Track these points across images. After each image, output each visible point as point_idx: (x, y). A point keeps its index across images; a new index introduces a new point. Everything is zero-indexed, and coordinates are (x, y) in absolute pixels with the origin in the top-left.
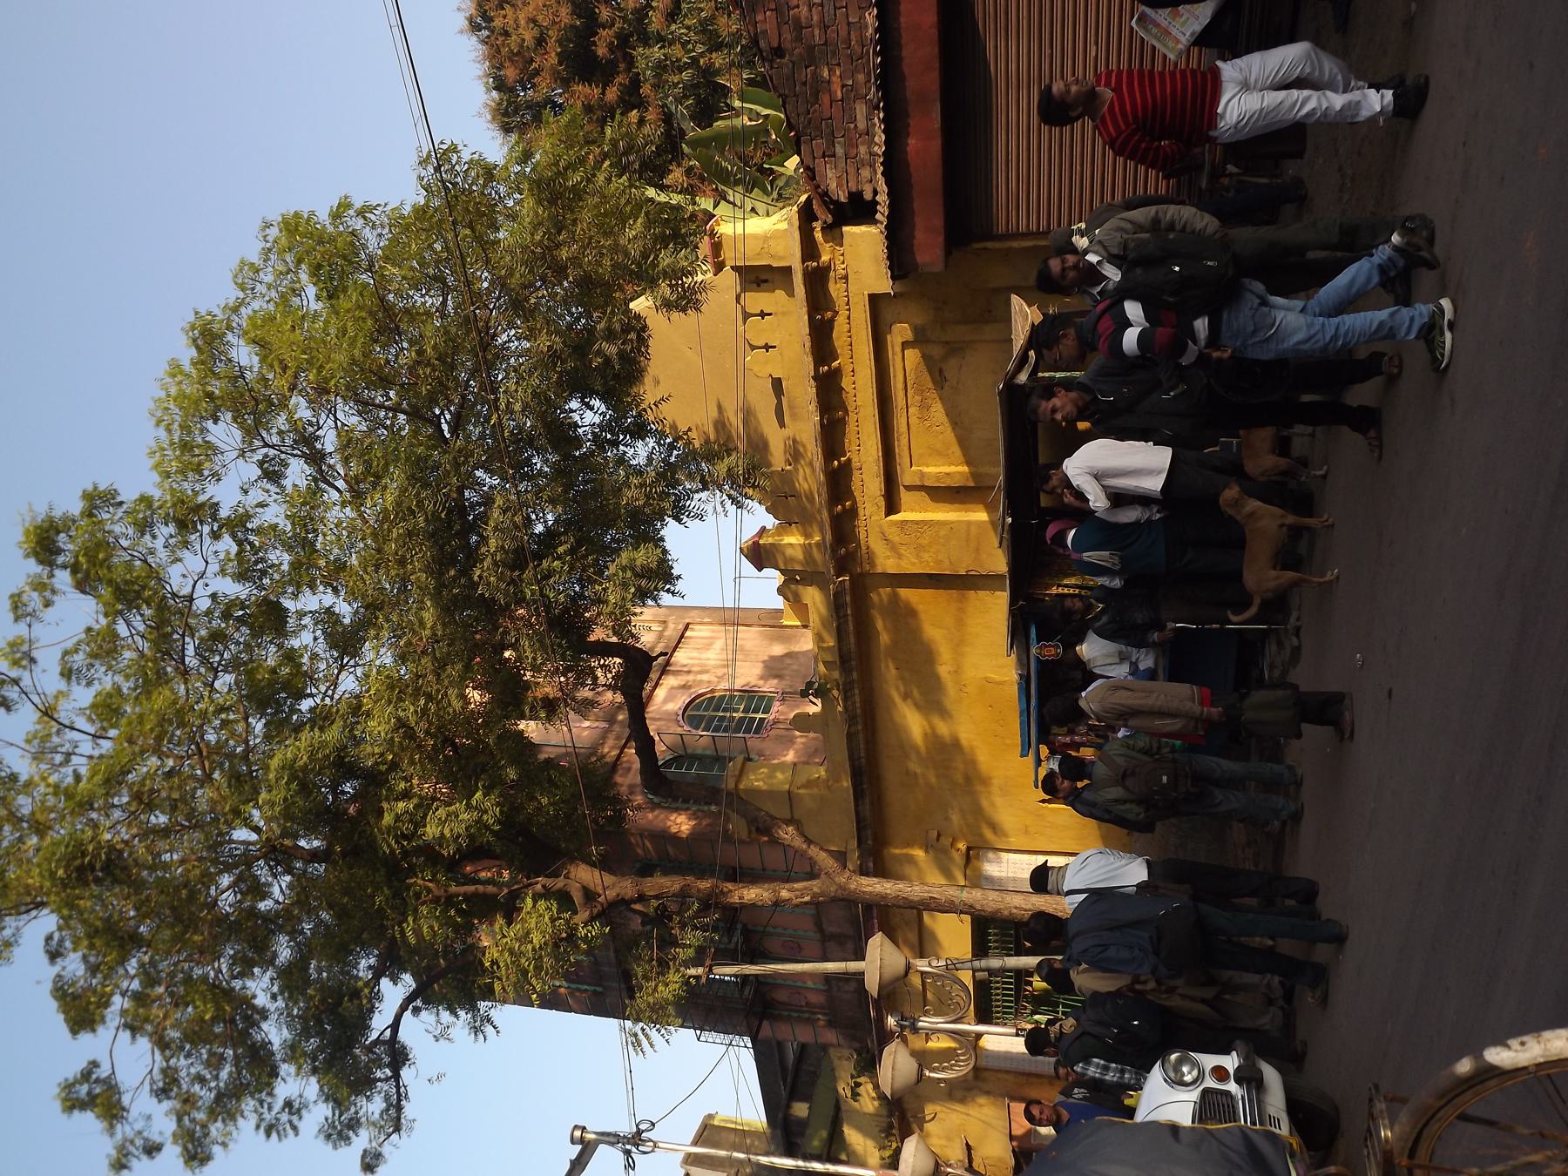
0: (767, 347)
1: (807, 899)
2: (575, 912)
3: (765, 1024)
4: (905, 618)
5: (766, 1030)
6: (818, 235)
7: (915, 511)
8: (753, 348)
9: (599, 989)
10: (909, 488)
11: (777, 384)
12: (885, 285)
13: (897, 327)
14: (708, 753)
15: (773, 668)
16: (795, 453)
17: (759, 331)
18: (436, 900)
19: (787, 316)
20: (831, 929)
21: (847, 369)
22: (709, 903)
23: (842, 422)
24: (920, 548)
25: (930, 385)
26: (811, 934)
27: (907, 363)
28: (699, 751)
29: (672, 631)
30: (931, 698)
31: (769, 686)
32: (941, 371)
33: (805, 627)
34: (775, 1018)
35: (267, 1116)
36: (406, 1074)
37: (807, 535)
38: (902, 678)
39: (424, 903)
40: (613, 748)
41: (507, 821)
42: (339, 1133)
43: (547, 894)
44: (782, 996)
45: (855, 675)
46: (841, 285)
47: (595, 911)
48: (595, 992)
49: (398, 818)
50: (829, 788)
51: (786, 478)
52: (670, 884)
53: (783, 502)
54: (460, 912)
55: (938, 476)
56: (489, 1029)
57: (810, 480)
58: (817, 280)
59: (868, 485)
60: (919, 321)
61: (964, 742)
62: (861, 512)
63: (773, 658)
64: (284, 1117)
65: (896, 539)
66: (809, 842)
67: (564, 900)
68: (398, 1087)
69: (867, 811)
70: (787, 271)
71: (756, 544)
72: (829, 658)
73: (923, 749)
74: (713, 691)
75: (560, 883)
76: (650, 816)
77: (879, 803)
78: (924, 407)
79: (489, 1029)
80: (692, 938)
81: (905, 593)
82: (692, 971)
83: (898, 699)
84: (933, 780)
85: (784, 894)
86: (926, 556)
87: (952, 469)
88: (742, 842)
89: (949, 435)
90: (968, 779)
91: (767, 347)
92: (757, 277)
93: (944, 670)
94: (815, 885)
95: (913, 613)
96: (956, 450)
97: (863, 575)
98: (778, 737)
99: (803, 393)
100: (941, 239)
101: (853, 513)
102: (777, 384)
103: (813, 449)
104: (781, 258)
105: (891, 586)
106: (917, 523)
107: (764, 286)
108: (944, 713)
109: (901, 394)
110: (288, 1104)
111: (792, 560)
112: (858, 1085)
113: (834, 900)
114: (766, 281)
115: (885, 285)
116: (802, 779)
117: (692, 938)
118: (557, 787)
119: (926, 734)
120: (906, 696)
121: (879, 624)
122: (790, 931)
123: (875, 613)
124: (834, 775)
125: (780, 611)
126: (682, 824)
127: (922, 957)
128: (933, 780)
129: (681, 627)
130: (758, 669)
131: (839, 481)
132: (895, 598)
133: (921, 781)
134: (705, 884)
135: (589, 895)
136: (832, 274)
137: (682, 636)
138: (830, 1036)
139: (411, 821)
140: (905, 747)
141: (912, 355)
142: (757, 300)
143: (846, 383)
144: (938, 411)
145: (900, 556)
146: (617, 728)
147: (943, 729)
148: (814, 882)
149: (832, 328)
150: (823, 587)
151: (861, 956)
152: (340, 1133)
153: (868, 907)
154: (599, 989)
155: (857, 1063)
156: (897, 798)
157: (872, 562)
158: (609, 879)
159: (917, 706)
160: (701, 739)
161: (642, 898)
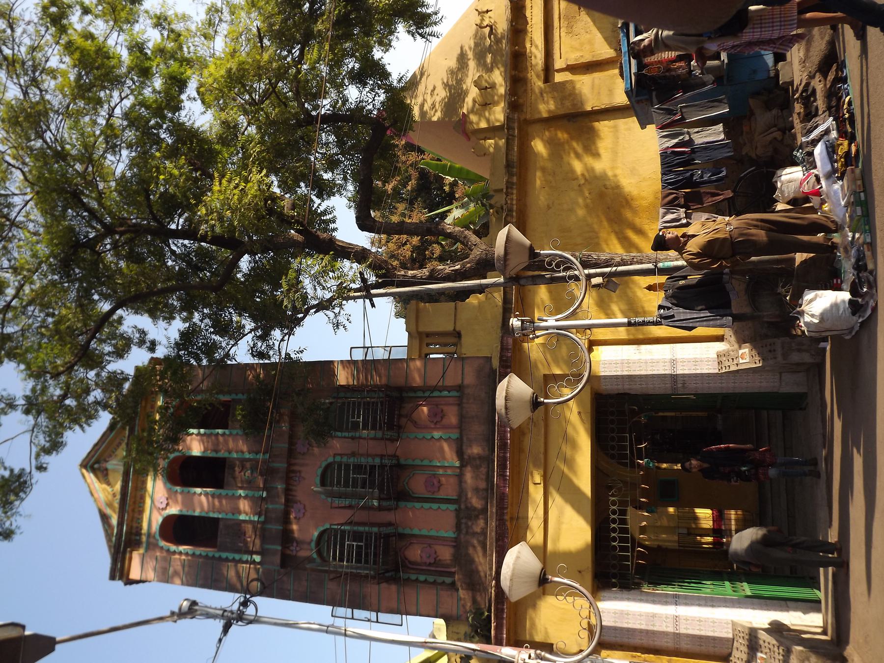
44: (415, 553)
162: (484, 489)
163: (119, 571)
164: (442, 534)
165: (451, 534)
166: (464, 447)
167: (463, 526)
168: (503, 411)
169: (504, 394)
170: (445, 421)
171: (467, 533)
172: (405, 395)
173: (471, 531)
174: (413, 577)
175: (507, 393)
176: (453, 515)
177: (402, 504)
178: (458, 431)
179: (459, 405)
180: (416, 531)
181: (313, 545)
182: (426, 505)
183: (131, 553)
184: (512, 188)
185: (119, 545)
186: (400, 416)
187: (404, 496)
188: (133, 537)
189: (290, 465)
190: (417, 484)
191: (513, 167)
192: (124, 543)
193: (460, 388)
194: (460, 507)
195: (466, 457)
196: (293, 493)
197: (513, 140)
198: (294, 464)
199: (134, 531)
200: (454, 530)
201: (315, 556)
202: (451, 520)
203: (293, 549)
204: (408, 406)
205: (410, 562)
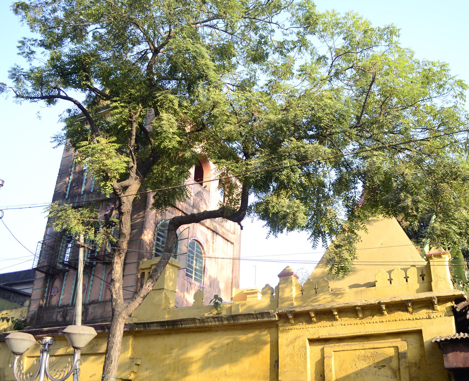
0: (390, 280)
1: (114, 296)
2: (119, 181)
3: (43, 275)
4: (255, 347)
5: (40, 275)
6: (449, 304)
7: (313, 353)
8: (390, 272)
10: (323, 350)
11: (373, 285)
12: (427, 337)
13: (405, 343)
14: (178, 251)
15: (214, 283)
16: (336, 293)
17: (398, 276)
18: (131, 117)
19: (410, 290)
21: (383, 318)
22: (115, 247)
23: (357, 316)
24: (292, 356)
25: (376, 361)
26: (88, 298)
27: (387, 349)
28: (179, 246)
29: (230, 237)
30: (209, 362)
31: (206, 280)
32: (384, 366)
33: (232, 299)
35: (29, 43)
36: (42, 103)
37: (296, 298)
38: (222, 347)
39: (130, 111)
40: (182, 206)
41: (165, 152)
42: (15, 75)
43: (129, 168)
44: (57, 283)
45: (226, 322)
46: (425, 316)
47: (118, 191)
48: (65, 194)
49: (171, 101)
50: (165, 309)
51: (325, 289)
52: (126, 229)
53: (313, 286)
54: (123, 127)
55: (330, 365)
56: (56, 144)
57: (324, 301)
58: (428, 304)
59: (324, 329)
60: (409, 355)
62: (310, 326)
63: (218, 283)
64: (27, 50)
65: (296, 344)
66: (144, 298)
67: (124, 177)
68: (38, 98)
69: (154, 328)
70: (430, 290)
71: (292, 274)
72: (233, 309)
73: (184, 357)
74: (205, 253)
75: (133, 174)
76: (152, 222)
77: (158, 334)
78: (365, 358)
79: (56, 144)
80: (100, 239)
81: (267, 349)
82: (82, 238)
84: (168, 362)
85: (117, 285)
86: (288, 359)
87: (334, 373)
88: (138, 264)
89: (351, 371)
91: (390, 280)
92: (425, 275)
93: (226, 368)
94: (121, 301)
95: (256, 351)
96: (343, 374)
97: (277, 327)
98: (184, 285)
99: (370, 297)
100: (461, 366)
101: (310, 321)
102: (373, 285)
103: (340, 302)
104: (436, 287)
105: (271, 341)
106: (305, 354)
107: (421, 277)
108: (202, 368)
109: (372, 346)
110: (33, 52)
111: (283, 291)
112: (8, 321)
113: (113, 310)
114: (423, 279)
115: (427, 337)
116: (169, 295)
117: (100, 239)
118: (179, 175)
119: (192, 358)
120: (213, 349)
121: (251, 335)
122: (90, 288)
123: (257, 332)
124: (170, 311)
125: (238, 288)
126: (148, 236)
127: (82, 355)
128: (168, 362)
129: (232, 241)
130: (214, 276)
131: (326, 314)
132: (265, 343)
133: (167, 356)
134: (125, 245)
135: (125, 188)
136: (431, 311)
137: (228, 241)
138: (34, 307)
139: (169, 107)
140: (185, 348)
141: (391, 352)
142: (413, 274)
143: (376, 318)
144: (363, 365)
145: (288, 346)
146: (191, 208)
147: (194, 367)
148: (122, 300)
149: (403, 311)
150: (270, 306)
151: (85, 322)
152: (15, 75)
153: (109, 327)
155: (19, 321)
156: (158, 344)
157: (283, 331)
158: (131, 198)
159: (207, 354)
160: (183, 247)
161: (121, 214)
164: (62, 297)
166: (92, 305)
171: (58, 312)
178: (102, 300)
180: (64, 282)
184: (219, 321)
191: (234, 320)
194: (70, 306)
197: (254, 318)
205: (53, 282)
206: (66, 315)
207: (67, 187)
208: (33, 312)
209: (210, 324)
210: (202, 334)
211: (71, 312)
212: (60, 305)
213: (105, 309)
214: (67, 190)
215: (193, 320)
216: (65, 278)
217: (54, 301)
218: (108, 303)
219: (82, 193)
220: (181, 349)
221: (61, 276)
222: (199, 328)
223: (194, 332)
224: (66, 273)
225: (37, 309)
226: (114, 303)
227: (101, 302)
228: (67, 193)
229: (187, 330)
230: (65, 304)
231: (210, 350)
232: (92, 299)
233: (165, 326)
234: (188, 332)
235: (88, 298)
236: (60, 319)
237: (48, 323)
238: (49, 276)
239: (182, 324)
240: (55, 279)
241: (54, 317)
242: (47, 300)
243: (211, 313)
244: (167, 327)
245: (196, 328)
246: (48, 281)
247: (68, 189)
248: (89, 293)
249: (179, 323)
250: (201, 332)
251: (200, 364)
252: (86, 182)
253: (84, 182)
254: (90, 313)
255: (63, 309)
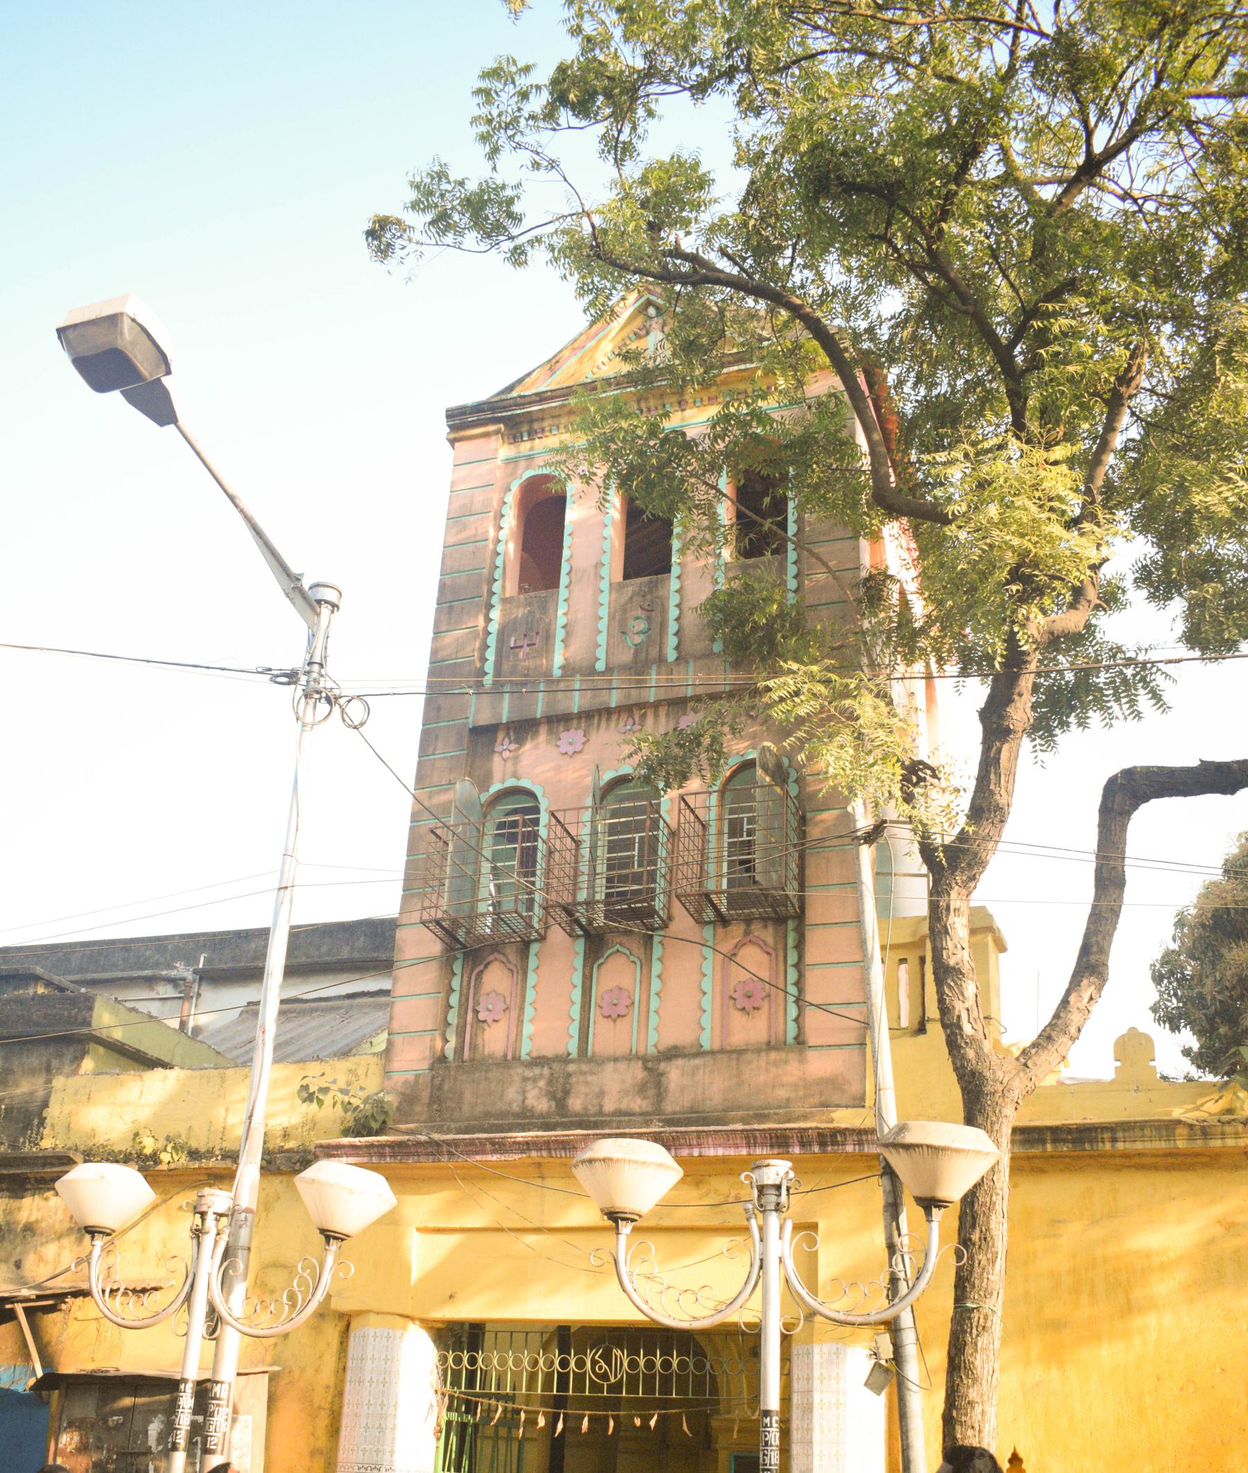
1: (967, 1029)
9: (488, 680)
20: (675, 1073)
26: (653, 1038)
34: (447, 961)
44: (496, 978)
61: (1138, 1321)
83: (1219, 1210)
90: (1054, 1326)
122: (655, 1003)
154: (488, 680)
159: (1211, 1241)
162: (601, 1106)
163: (462, 421)
164: (528, 1029)
165: (526, 1049)
166: (680, 1062)
167: (537, 1071)
168: (588, 1155)
169: (615, 1155)
170: (737, 1019)
171: (525, 1079)
172: (791, 925)
173: (529, 1087)
174: (456, 983)
175: (617, 1160)
176: (560, 1050)
177: (580, 945)
178: (717, 1047)
179: (768, 1043)
180: (532, 978)
181: (511, 782)
182: (577, 995)
183: (497, 432)
185: (505, 409)
186: (748, 921)
187: (596, 945)
188: (525, 428)
189: (656, 705)
190: (617, 972)
192: (507, 416)
193: (800, 1040)
194: (573, 1061)
195: (663, 1066)
196: (603, 724)
198: (656, 716)
199: (536, 426)
200: (534, 1054)
201: (495, 787)
202: (550, 1049)
203: (504, 745)
204: (767, 935)
205: (482, 972)
206: (567, 1093)
207: (485, 647)
208: (410, 1077)
209: (1230, 1142)
210: (1176, 1175)
211: (587, 1083)
212: (524, 1057)
213: (738, 1076)
214: (483, 660)
215: (1168, 1127)
216: (533, 962)
217: (494, 1040)
218: (749, 1056)
219: (557, 673)
220: (1094, 1222)
221: (512, 956)
222: (1185, 1154)
223: (1142, 1167)
224: (534, 948)
225: (425, 1065)
226: (971, 1054)
227: (712, 1053)
228: (489, 667)
229: (1118, 1161)
230: (549, 1053)
231: (1219, 1230)
232: (669, 1040)
233: (1044, 1142)
234: (1118, 1169)
235: (653, 1038)
236: (539, 1102)
237: (487, 1114)
238: (459, 955)
239: (1114, 1140)
240: (486, 967)
241: (512, 1094)
242: (461, 1034)
243: (1198, 1108)
244: (1049, 1147)
245: (1157, 1156)
246: (457, 967)
247: (491, 655)
248: (654, 1020)
249: (1106, 1136)
250: (1168, 1168)
251: (1181, 1276)
252: (568, 634)
253: (560, 634)
254: (672, 1086)
255: (546, 1071)
